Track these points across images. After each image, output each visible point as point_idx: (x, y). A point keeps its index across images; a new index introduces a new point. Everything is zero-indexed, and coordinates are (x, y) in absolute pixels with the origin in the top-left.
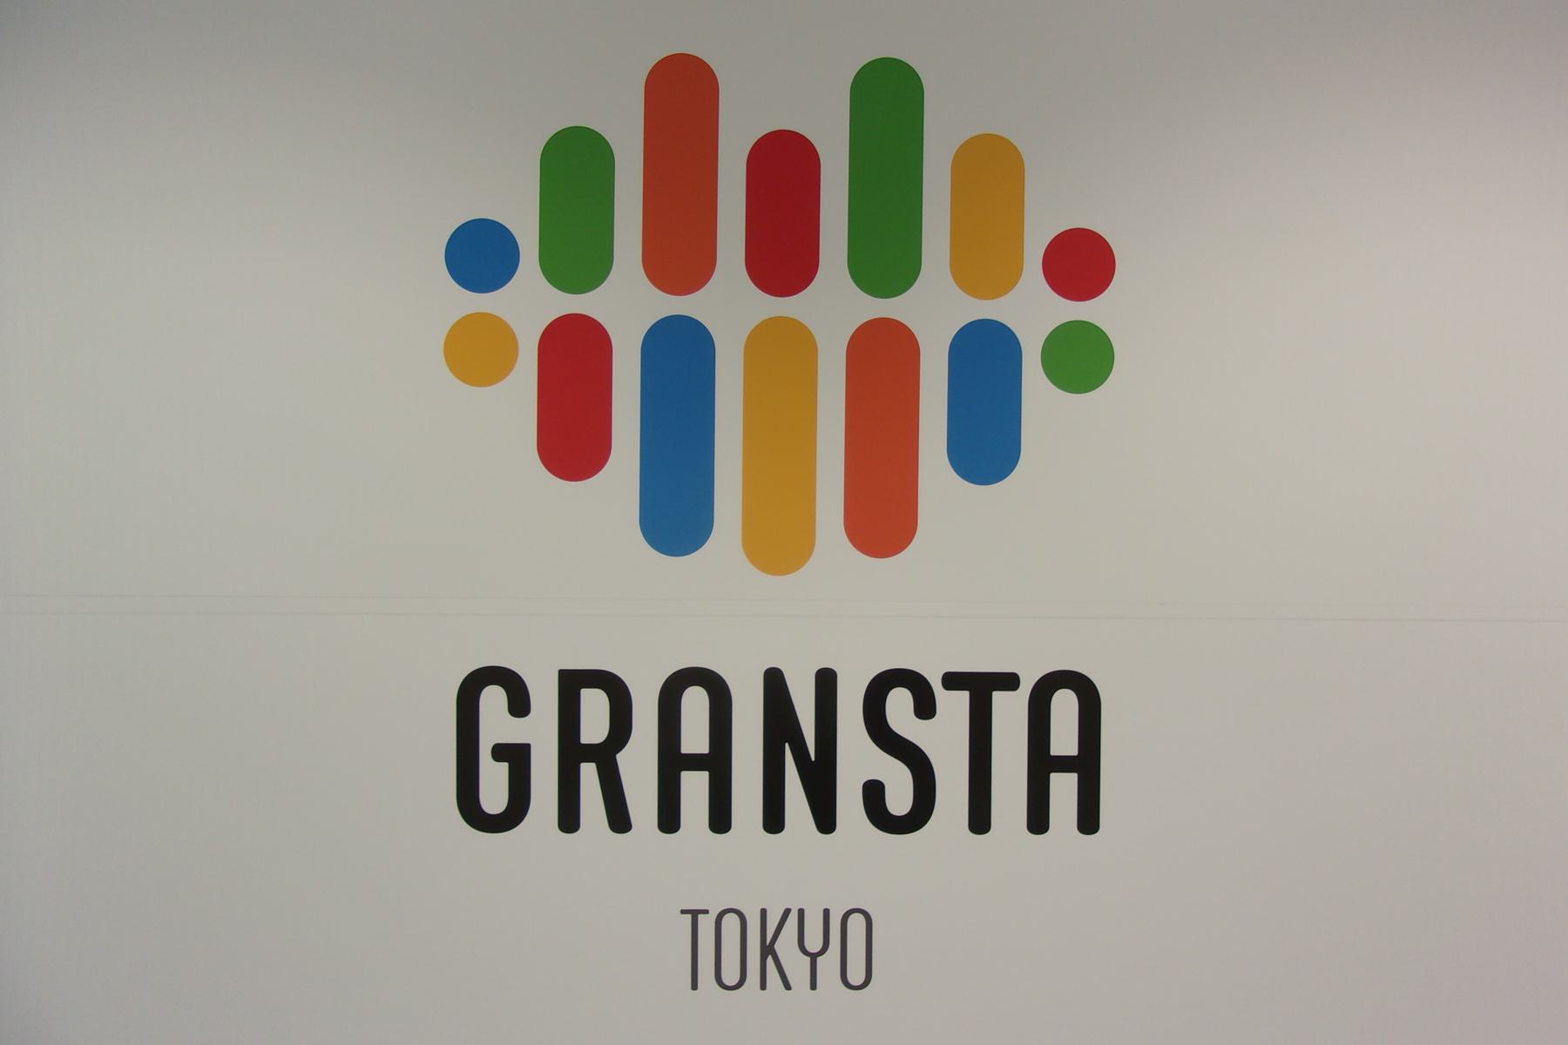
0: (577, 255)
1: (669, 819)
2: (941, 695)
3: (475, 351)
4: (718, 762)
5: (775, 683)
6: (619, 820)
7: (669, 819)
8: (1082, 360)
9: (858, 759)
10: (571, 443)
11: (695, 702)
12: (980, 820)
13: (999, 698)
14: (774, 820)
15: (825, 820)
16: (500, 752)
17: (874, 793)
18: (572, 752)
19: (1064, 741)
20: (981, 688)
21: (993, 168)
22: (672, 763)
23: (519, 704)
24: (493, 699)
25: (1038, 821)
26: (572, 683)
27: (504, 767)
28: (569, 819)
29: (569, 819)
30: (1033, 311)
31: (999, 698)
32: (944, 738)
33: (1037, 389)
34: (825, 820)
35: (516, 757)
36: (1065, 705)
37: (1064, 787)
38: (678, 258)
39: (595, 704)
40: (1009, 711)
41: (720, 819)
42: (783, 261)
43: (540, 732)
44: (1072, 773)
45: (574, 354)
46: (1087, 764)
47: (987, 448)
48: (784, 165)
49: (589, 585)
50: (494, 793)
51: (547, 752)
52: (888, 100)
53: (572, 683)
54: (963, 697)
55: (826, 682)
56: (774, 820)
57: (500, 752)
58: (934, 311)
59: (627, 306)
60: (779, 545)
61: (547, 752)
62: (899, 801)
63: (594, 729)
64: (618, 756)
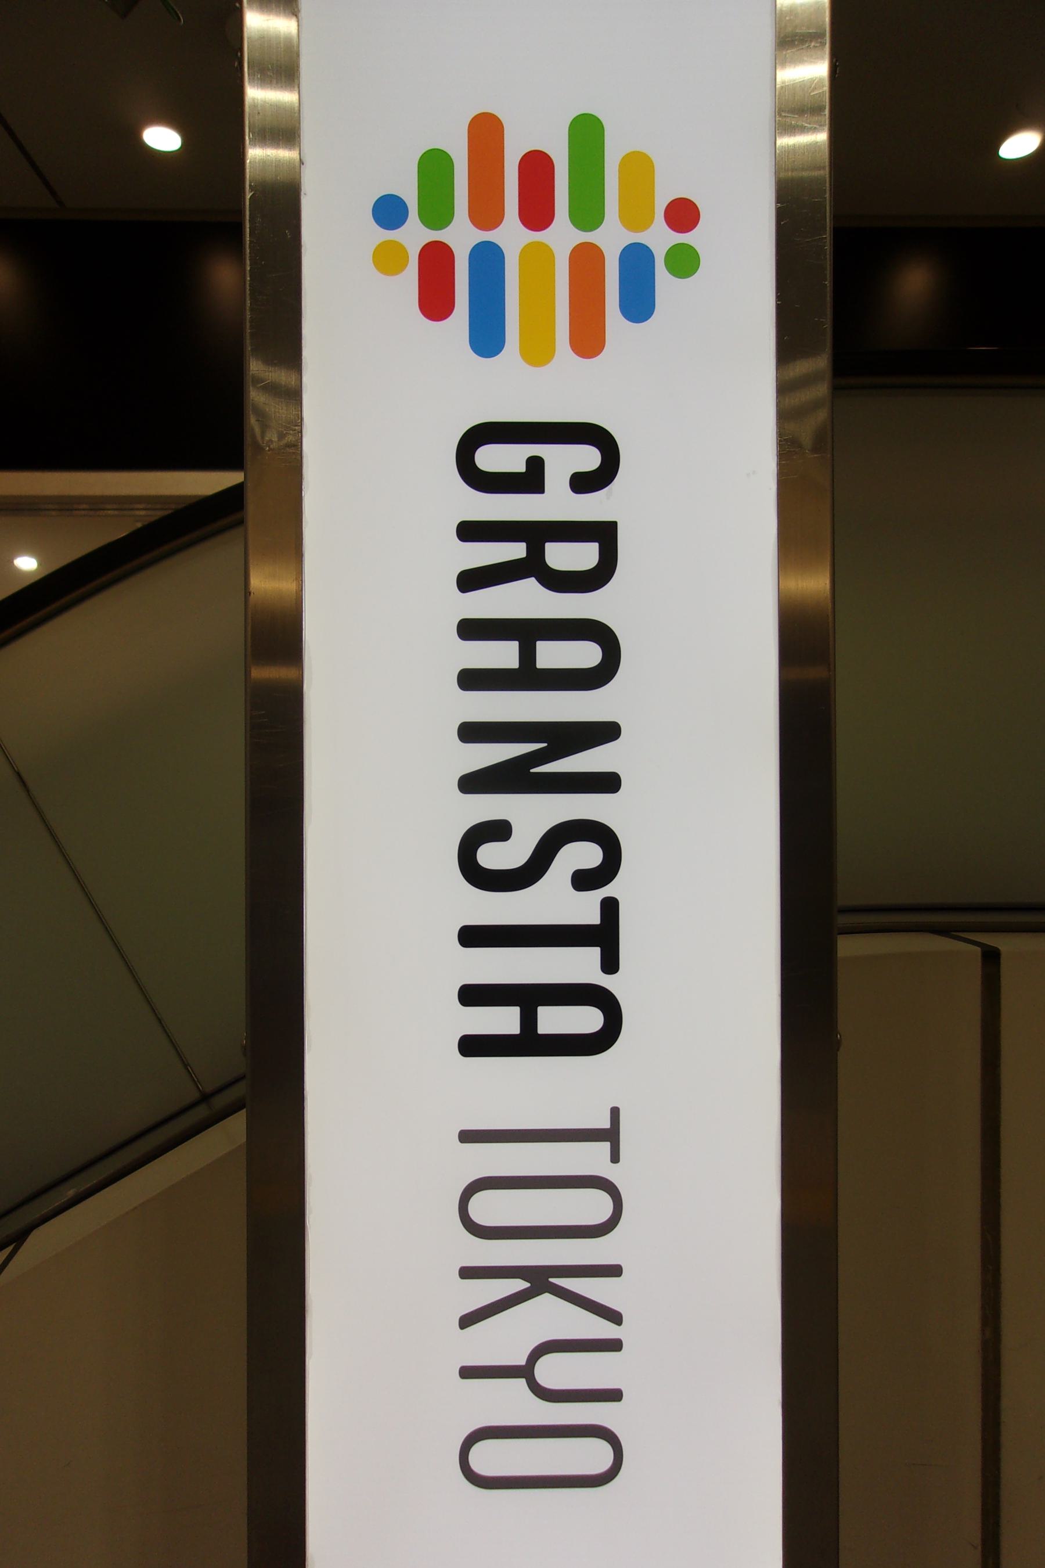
1: (471, 629)
4: (527, 677)
5: (606, 732)
6: (471, 580)
7: (471, 629)
9: (532, 815)
11: (585, 655)
12: (473, 936)
13: (594, 953)
14: (472, 732)
15: (474, 783)
16: (536, 465)
17: (498, 831)
18: (537, 534)
19: (553, 1020)
20: (604, 936)
22: (527, 632)
23: (582, 483)
24: (588, 458)
25: (473, 995)
26: (604, 534)
27: (521, 468)
28: (469, 531)
29: (469, 531)
31: (594, 953)
32: (554, 900)
34: (474, 783)
35: (532, 479)
36: (587, 1020)
37: (505, 1020)
40: (579, 965)
41: (472, 680)
43: (556, 503)
46: (529, 1043)
50: (494, 458)
53: (604, 534)
54: (594, 918)
55: (607, 783)
56: (472, 732)
57: (536, 465)
62: (493, 856)
63: (564, 556)
64: (533, 579)
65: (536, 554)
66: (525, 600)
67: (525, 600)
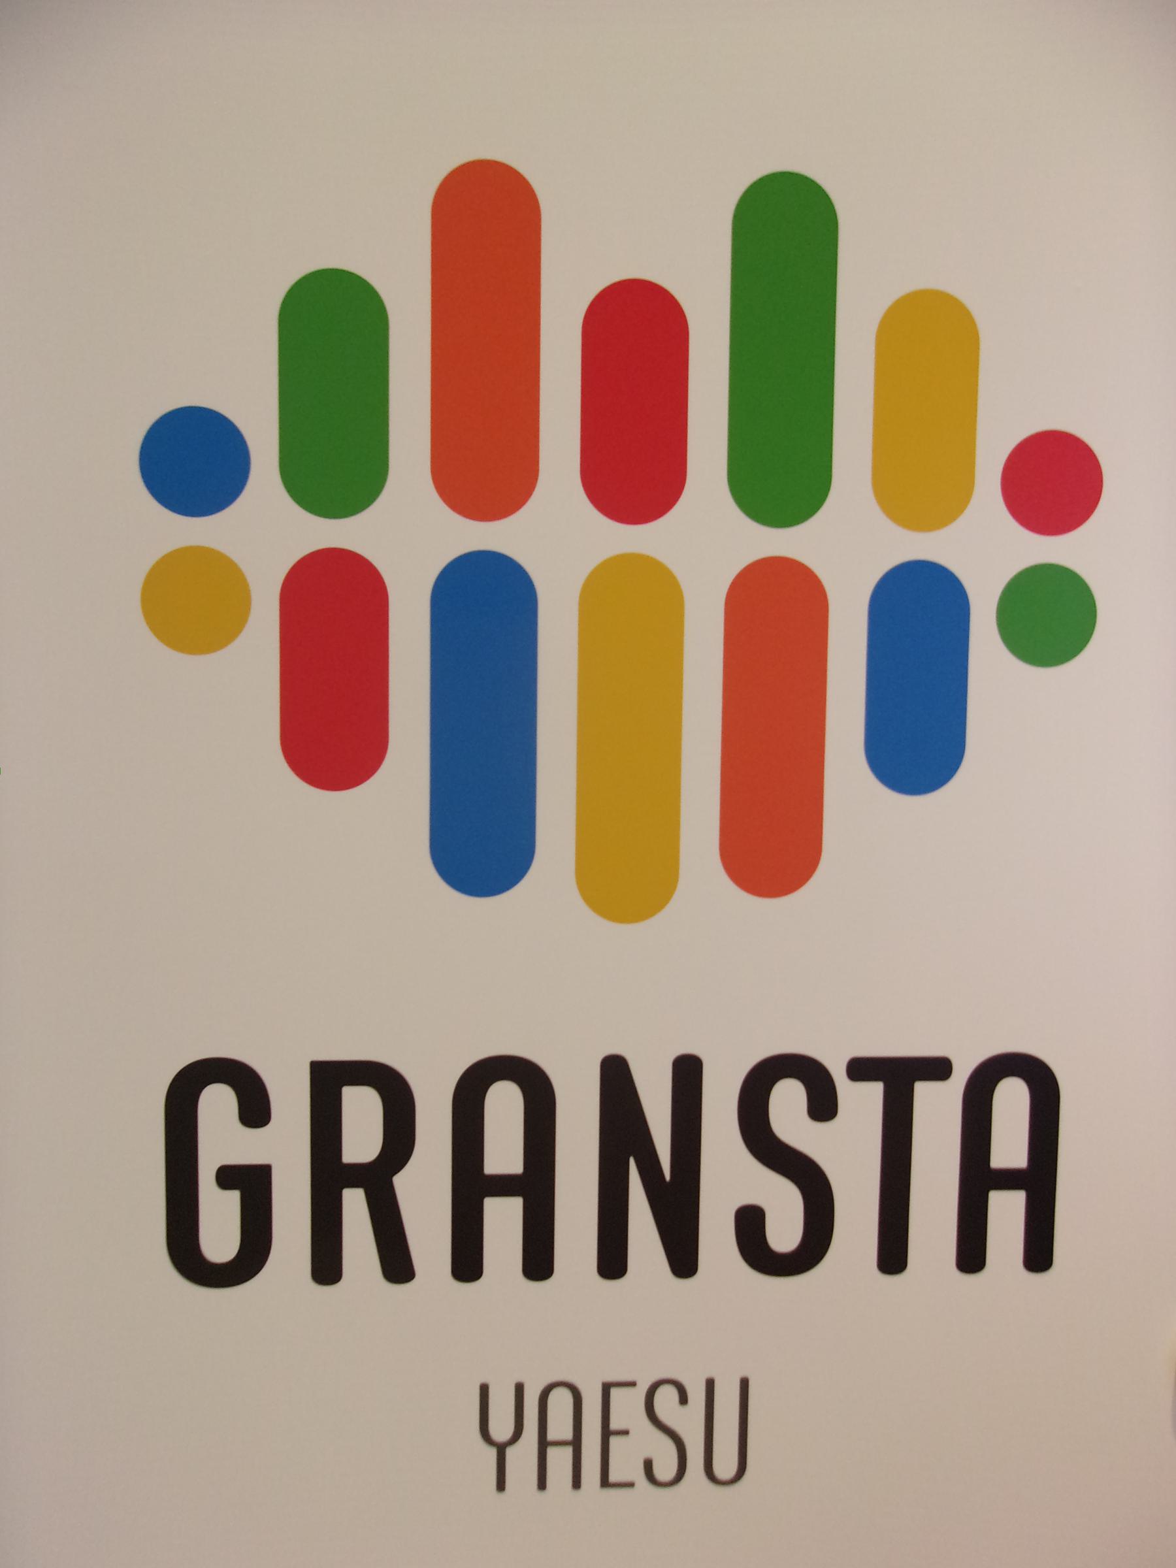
0: (335, 460)
1: (467, 1263)
2: (845, 1088)
3: (187, 605)
4: (536, 1186)
5: (616, 1076)
6: (397, 1264)
7: (467, 1263)
8: (1051, 619)
9: (730, 1177)
10: (329, 736)
11: (504, 1105)
12: (893, 1255)
13: (924, 1091)
14: (612, 1260)
15: (684, 1262)
16: (228, 1177)
17: (750, 1224)
18: (329, 1174)
19: (1010, 1148)
20: (899, 1077)
21: (935, 334)
22: (471, 1186)
23: (255, 1108)
24: (217, 1104)
25: (971, 1254)
26: (329, 1080)
27: (233, 1198)
28: (327, 1265)
29: (327, 1265)
30: (987, 550)
31: (924, 1091)
32: (847, 1148)
33: (990, 664)
34: (684, 1262)
35: (251, 1183)
36: (1012, 1100)
37: (1007, 1211)
38: (484, 465)
39: (362, 1112)
40: (937, 1110)
41: (538, 1261)
42: (634, 471)
43: (284, 1148)
44: (1018, 1189)
45: (332, 608)
46: (1039, 1180)
47: (919, 742)
48: (635, 328)
49: (349, 938)
50: (220, 1236)
51: (282, 1174)
52: (785, 234)
53: (329, 1080)
54: (873, 1093)
55: (688, 1074)
56: (612, 1260)
57: (228, 1177)
58: (849, 547)
59: (410, 536)
60: (627, 884)
61: (282, 1174)
62: (785, 1232)
63: (362, 1137)
65: (358, 1175)
66: (425, 1191)
67: (425, 1191)
